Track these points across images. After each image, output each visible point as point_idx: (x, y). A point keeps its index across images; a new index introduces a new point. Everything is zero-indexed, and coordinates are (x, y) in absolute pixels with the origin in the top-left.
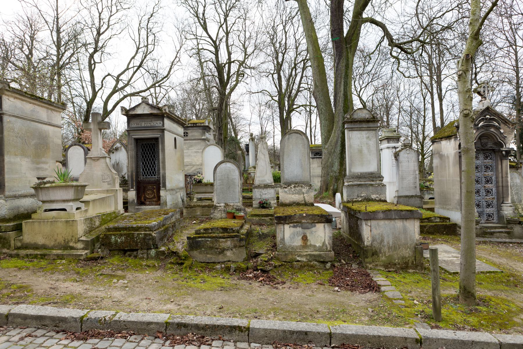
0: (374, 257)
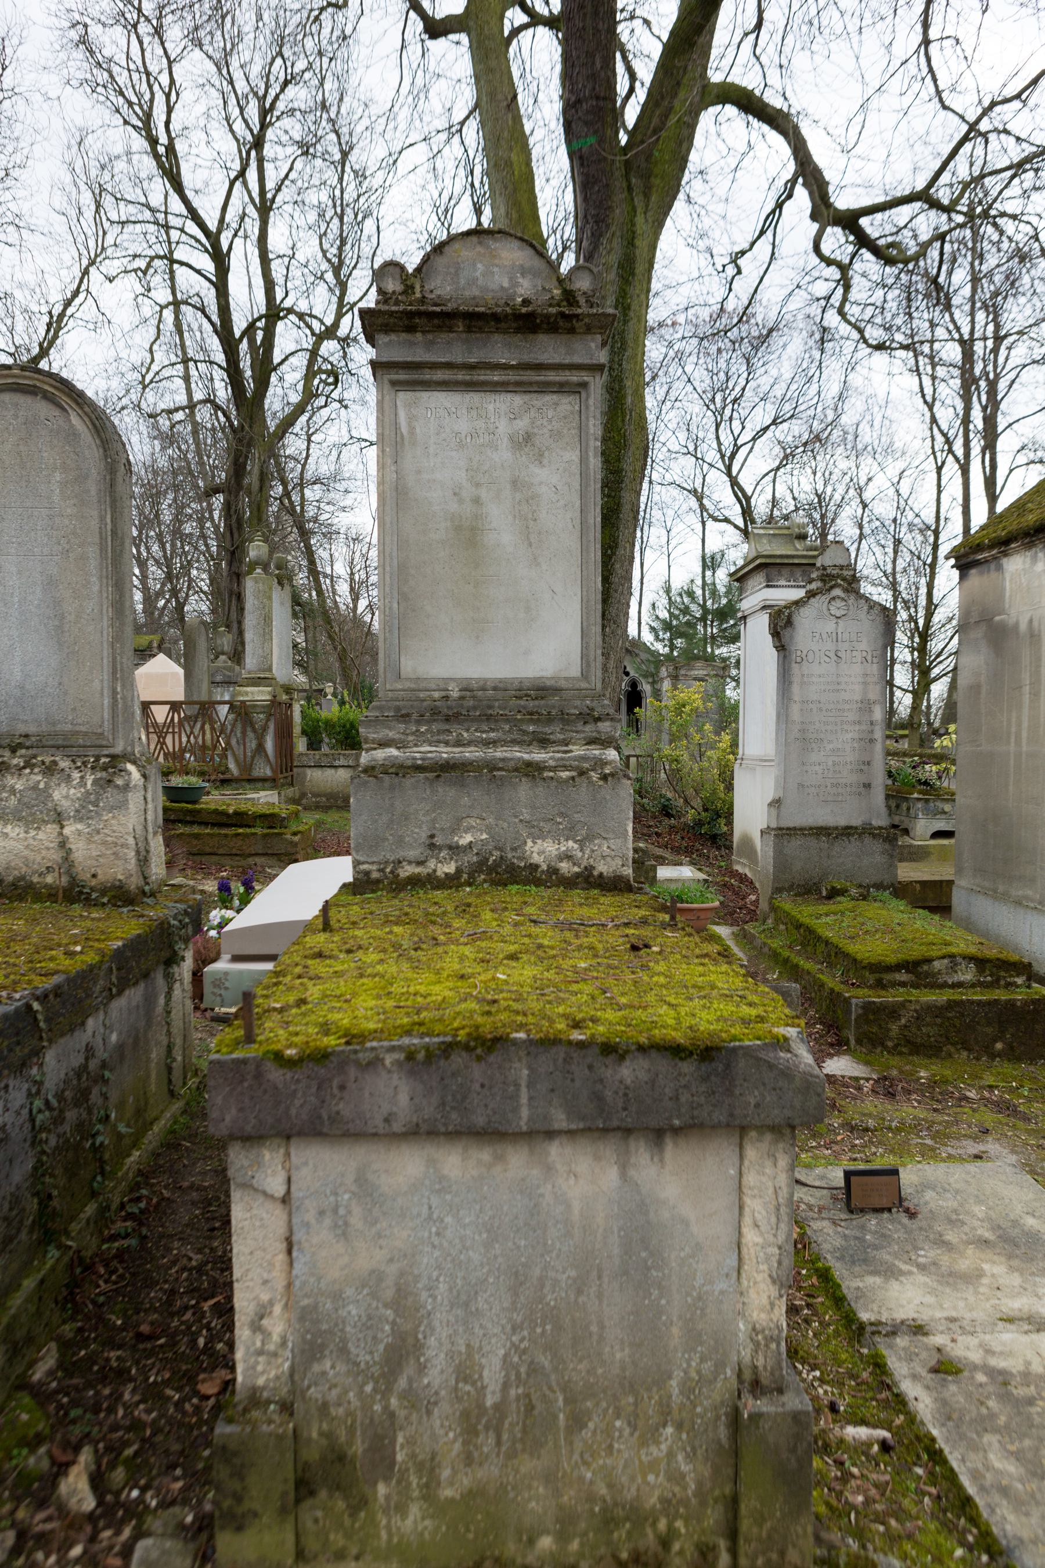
0: (312, 1513)
